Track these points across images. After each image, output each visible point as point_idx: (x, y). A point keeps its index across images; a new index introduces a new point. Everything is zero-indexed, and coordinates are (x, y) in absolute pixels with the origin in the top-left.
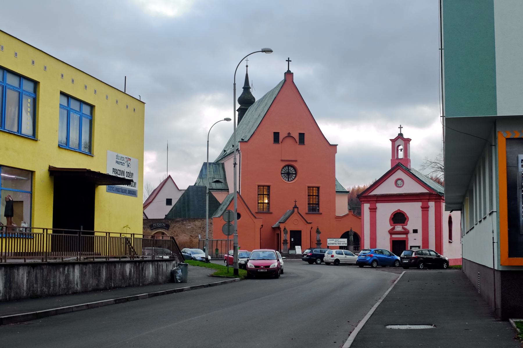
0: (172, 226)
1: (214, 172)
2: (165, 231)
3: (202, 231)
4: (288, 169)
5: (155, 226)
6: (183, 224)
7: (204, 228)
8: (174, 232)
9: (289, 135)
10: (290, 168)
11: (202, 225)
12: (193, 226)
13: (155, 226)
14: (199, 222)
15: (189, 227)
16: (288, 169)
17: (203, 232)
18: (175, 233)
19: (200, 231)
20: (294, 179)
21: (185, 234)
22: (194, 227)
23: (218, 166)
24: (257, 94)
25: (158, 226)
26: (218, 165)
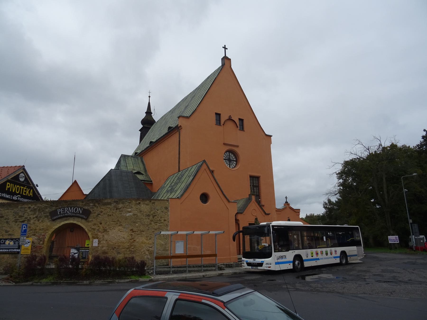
0: (95, 213)
1: (133, 165)
2: (81, 223)
3: (152, 221)
4: (229, 155)
5: (60, 213)
6: (117, 209)
7: (156, 216)
8: (99, 224)
9: (230, 119)
10: (231, 154)
11: (151, 210)
12: (136, 212)
13: (60, 213)
14: (147, 205)
15: (128, 214)
16: (229, 155)
17: (152, 223)
18: (100, 225)
19: (149, 221)
20: (235, 167)
21: (120, 228)
22: (139, 214)
23: (136, 159)
24: (156, 117)
25: (67, 213)
26: (136, 158)
